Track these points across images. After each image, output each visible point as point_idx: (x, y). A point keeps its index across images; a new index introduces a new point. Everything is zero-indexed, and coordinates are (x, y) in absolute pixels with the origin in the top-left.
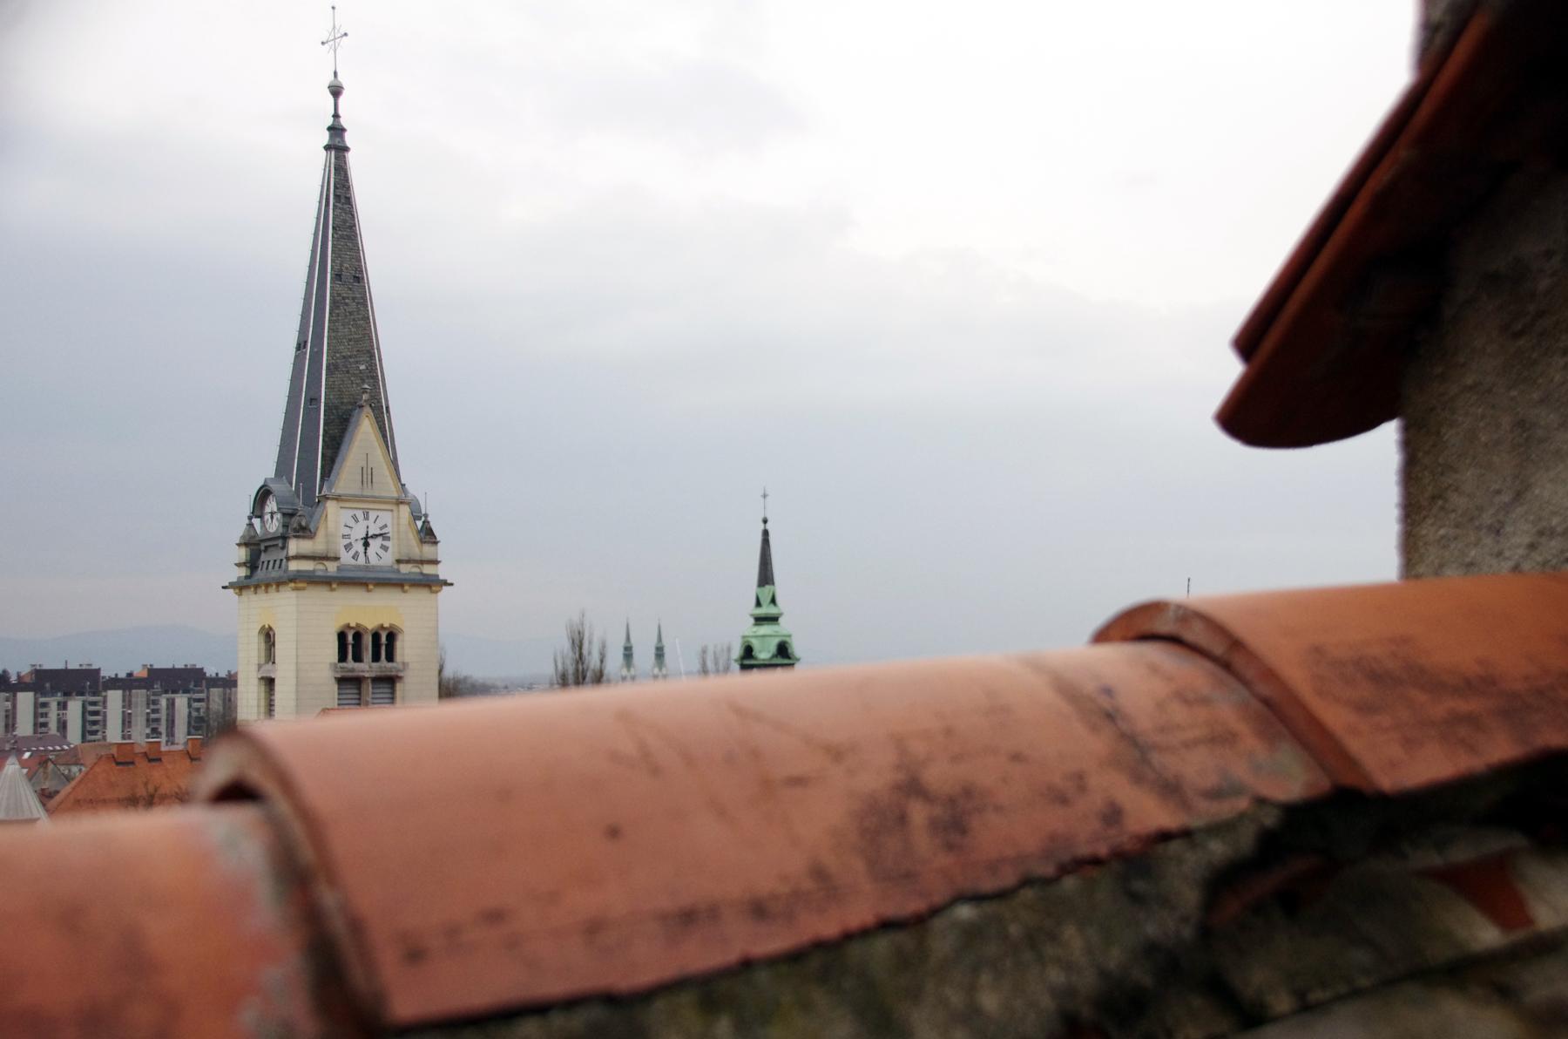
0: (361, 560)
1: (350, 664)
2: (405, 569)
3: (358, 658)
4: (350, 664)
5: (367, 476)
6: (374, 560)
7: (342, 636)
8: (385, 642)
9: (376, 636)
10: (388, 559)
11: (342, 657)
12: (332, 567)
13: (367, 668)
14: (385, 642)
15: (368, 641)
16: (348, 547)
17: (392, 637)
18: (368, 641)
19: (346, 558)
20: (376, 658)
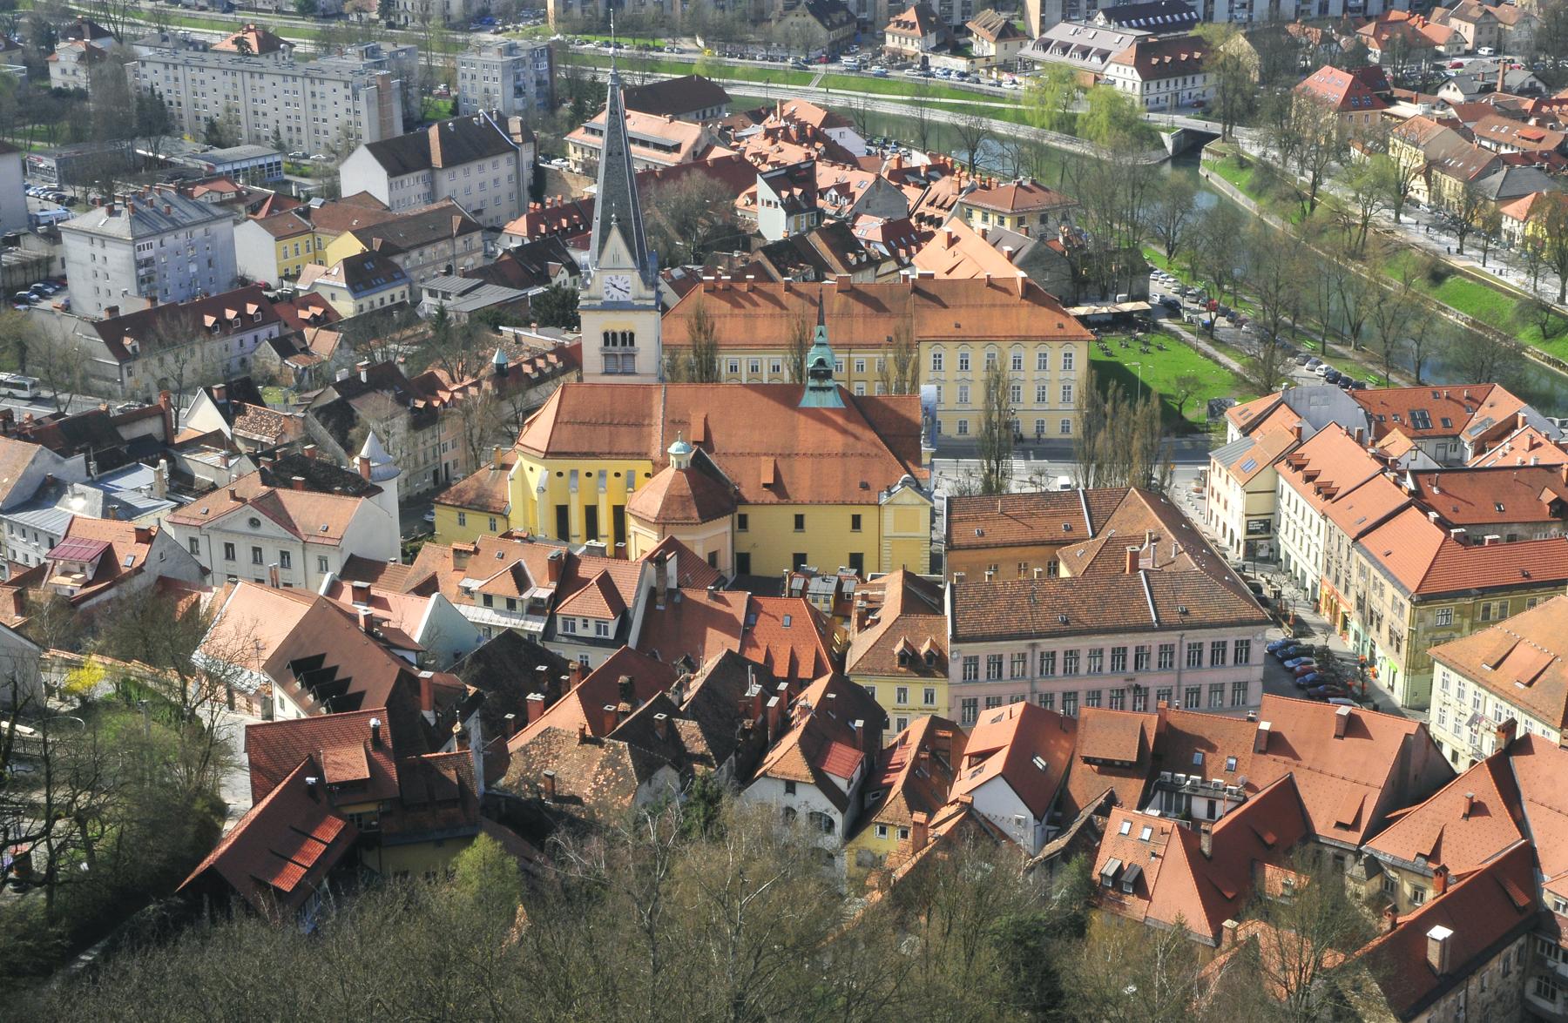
0: (615, 299)
1: (610, 346)
2: (636, 303)
3: (615, 344)
4: (610, 346)
5: (616, 258)
6: (621, 299)
7: (606, 335)
8: (628, 338)
9: (624, 334)
10: (628, 298)
11: (606, 343)
12: (598, 303)
13: (618, 349)
14: (628, 338)
15: (619, 338)
16: (608, 293)
17: (632, 335)
18: (619, 338)
19: (607, 298)
20: (624, 343)
